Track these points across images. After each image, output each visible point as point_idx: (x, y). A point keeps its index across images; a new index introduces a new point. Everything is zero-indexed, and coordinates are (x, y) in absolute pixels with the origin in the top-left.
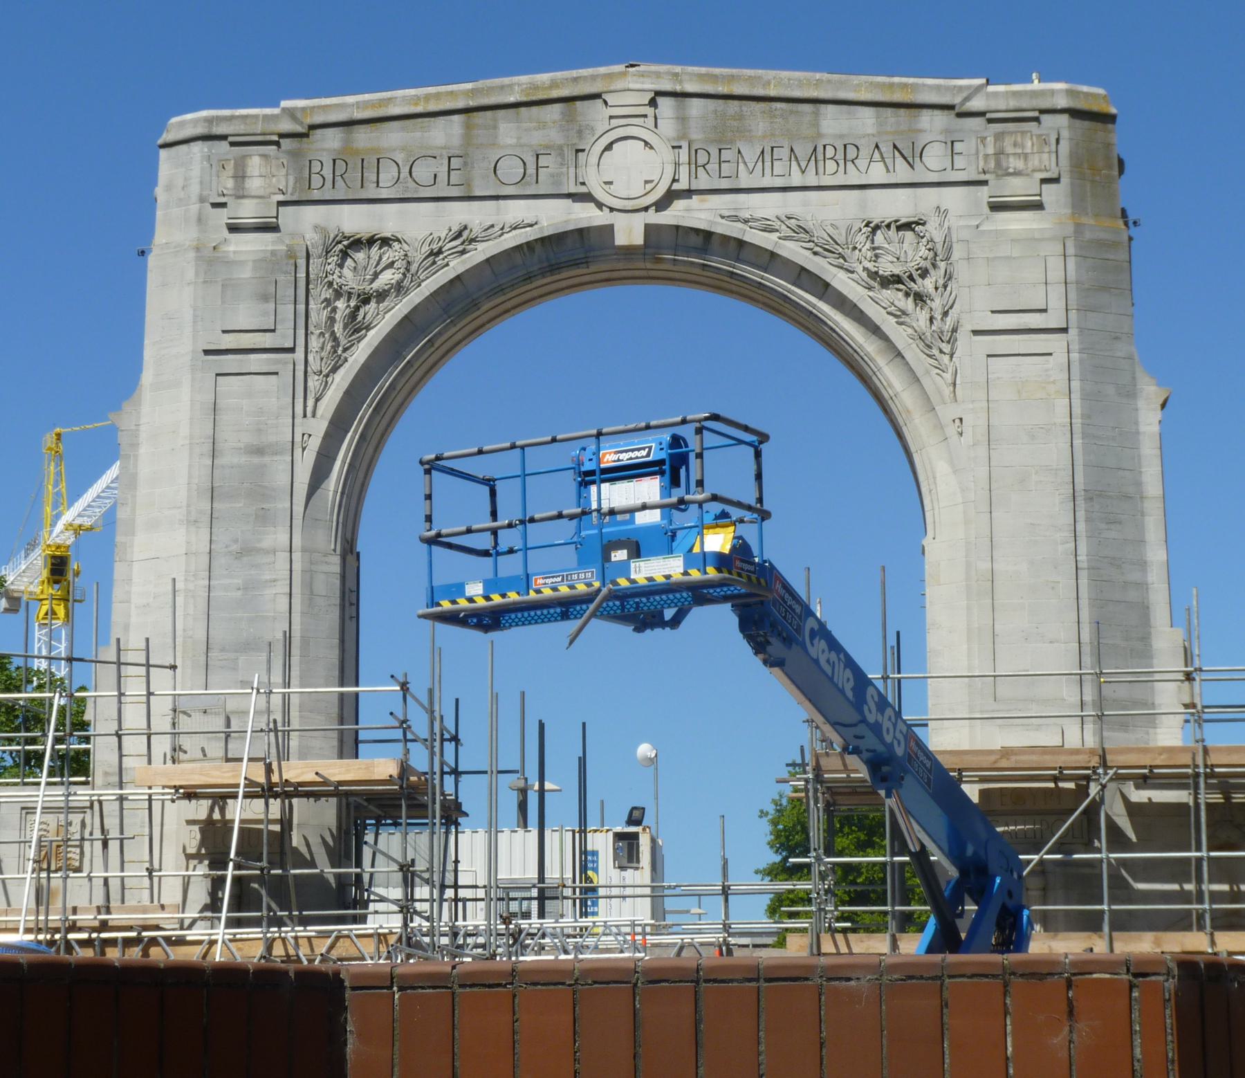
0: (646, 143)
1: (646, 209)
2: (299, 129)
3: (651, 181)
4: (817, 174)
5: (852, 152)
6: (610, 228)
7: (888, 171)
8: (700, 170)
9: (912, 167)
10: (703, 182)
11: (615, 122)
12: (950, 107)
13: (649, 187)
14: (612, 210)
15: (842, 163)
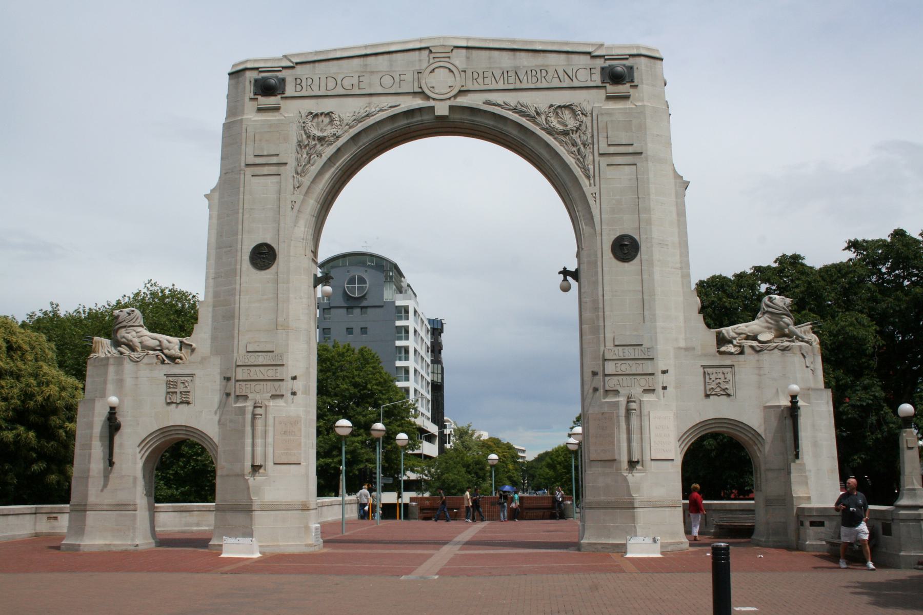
0: (449, 69)
1: (449, 99)
2: (291, 64)
3: (452, 86)
4: (528, 82)
5: (544, 73)
6: (433, 108)
7: (561, 82)
8: (475, 81)
9: (572, 80)
10: (476, 87)
11: (436, 60)
12: (589, 53)
13: (452, 88)
14: (434, 99)
15: (539, 78)
